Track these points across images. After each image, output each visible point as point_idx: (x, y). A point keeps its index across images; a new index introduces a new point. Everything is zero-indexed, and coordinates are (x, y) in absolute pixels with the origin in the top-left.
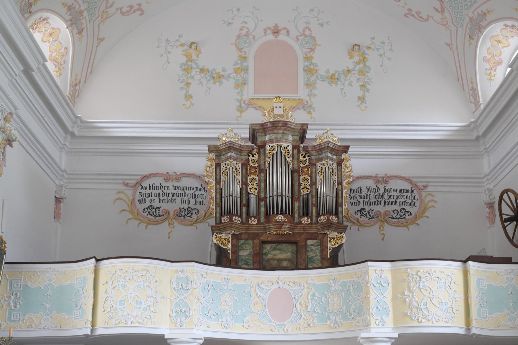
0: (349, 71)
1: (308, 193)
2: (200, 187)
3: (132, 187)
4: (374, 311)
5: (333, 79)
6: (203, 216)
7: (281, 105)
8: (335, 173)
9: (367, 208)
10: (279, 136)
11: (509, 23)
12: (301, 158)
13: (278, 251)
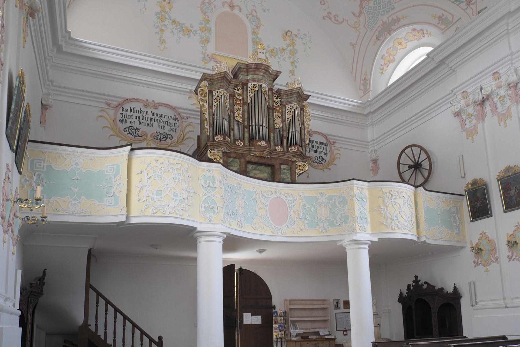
2: (173, 117)
3: (114, 108)
4: (358, 220)
6: (176, 141)
11: (418, 27)
12: (275, 99)
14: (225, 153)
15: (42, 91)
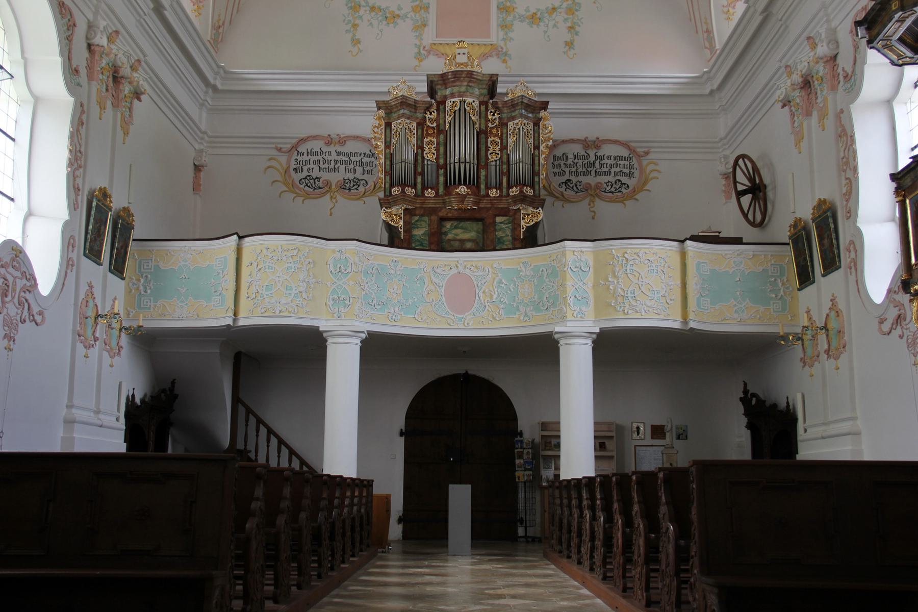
0: (554, 9)
1: (497, 159)
2: (368, 152)
4: (572, 301)
5: (534, 19)
7: (466, 51)
8: (531, 134)
9: (574, 179)
10: (463, 89)
13: (459, 230)
14: (406, 210)
15: (195, 149)
